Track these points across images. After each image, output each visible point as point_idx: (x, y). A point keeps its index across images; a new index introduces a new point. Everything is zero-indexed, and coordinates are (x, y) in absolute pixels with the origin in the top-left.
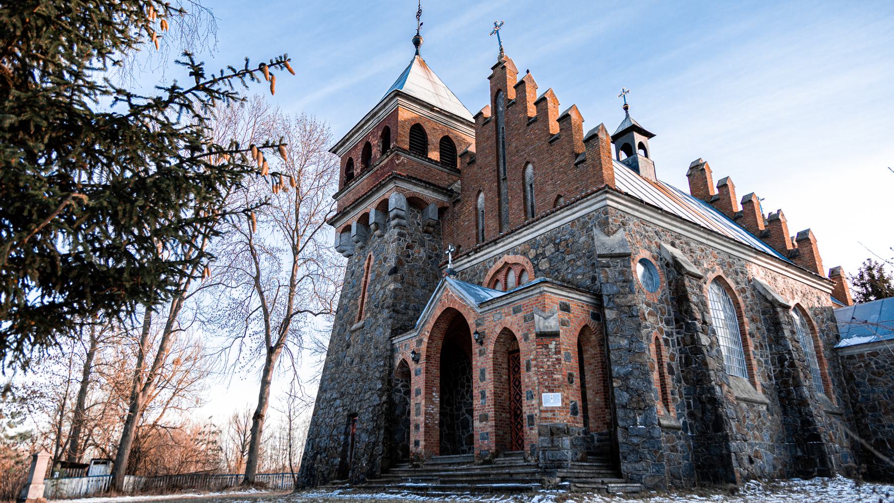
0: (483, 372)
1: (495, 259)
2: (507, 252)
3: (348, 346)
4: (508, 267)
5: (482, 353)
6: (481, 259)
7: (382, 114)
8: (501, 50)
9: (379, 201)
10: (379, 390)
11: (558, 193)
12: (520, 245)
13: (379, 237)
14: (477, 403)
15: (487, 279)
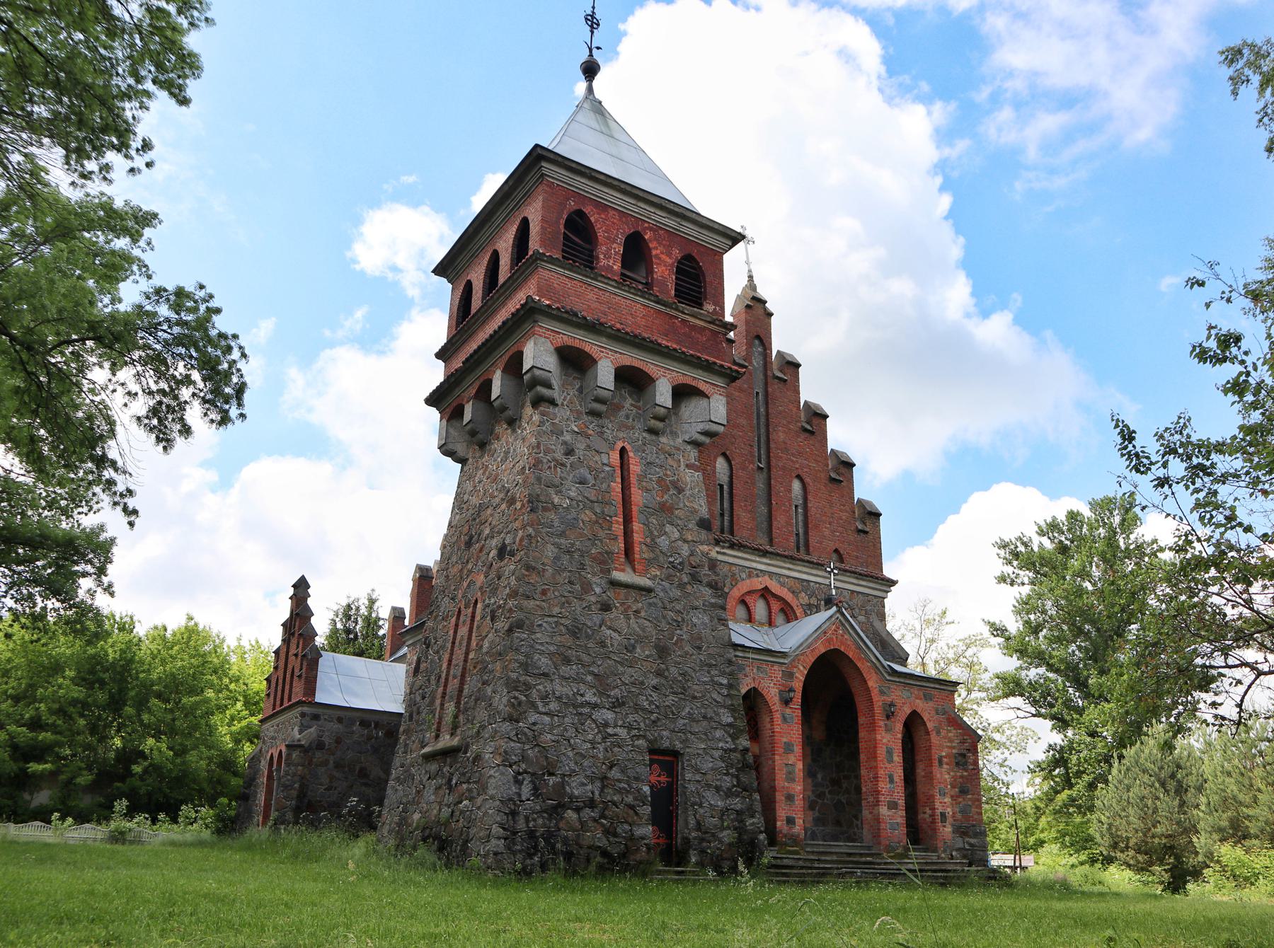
0: (890, 752)
1: (753, 573)
2: (771, 574)
3: (606, 607)
4: (765, 593)
5: (888, 729)
6: (731, 560)
7: (689, 230)
8: (751, 277)
9: (682, 380)
10: (730, 725)
11: (837, 546)
12: (788, 577)
13: (653, 431)
14: (884, 786)
15: (736, 593)
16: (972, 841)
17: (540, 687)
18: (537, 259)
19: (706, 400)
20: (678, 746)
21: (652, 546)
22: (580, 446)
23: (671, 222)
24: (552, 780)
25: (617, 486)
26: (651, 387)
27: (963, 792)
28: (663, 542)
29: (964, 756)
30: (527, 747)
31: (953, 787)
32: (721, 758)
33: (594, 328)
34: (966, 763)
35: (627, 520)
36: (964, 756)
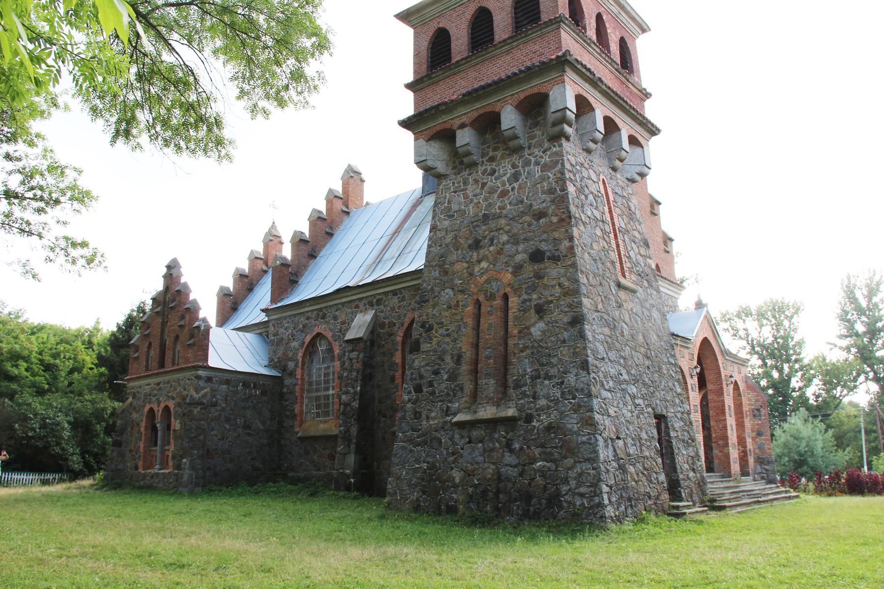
7: (624, 17)
16: (767, 467)
17: (603, 369)
18: (559, 22)
19: (640, 149)
20: (664, 412)
21: (629, 257)
22: (585, 175)
23: (615, 9)
24: (620, 443)
25: (606, 209)
26: (615, 135)
27: (759, 434)
28: (632, 254)
29: (758, 410)
30: (605, 417)
31: (753, 431)
32: (681, 418)
33: (595, 82)
34: (760, 415)
35: (615, 235)
36: (758, 410)
